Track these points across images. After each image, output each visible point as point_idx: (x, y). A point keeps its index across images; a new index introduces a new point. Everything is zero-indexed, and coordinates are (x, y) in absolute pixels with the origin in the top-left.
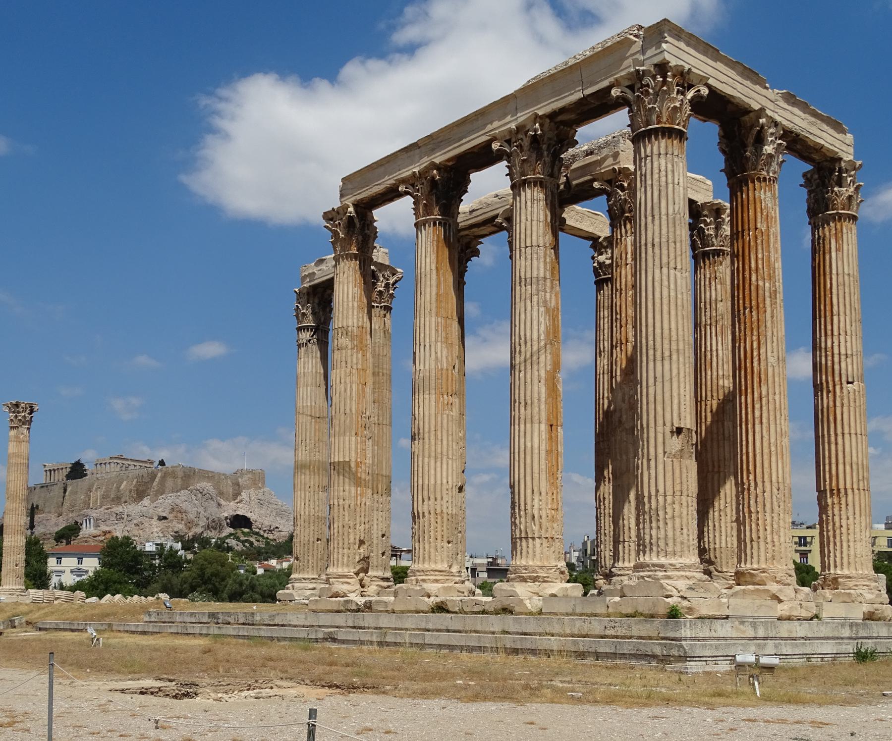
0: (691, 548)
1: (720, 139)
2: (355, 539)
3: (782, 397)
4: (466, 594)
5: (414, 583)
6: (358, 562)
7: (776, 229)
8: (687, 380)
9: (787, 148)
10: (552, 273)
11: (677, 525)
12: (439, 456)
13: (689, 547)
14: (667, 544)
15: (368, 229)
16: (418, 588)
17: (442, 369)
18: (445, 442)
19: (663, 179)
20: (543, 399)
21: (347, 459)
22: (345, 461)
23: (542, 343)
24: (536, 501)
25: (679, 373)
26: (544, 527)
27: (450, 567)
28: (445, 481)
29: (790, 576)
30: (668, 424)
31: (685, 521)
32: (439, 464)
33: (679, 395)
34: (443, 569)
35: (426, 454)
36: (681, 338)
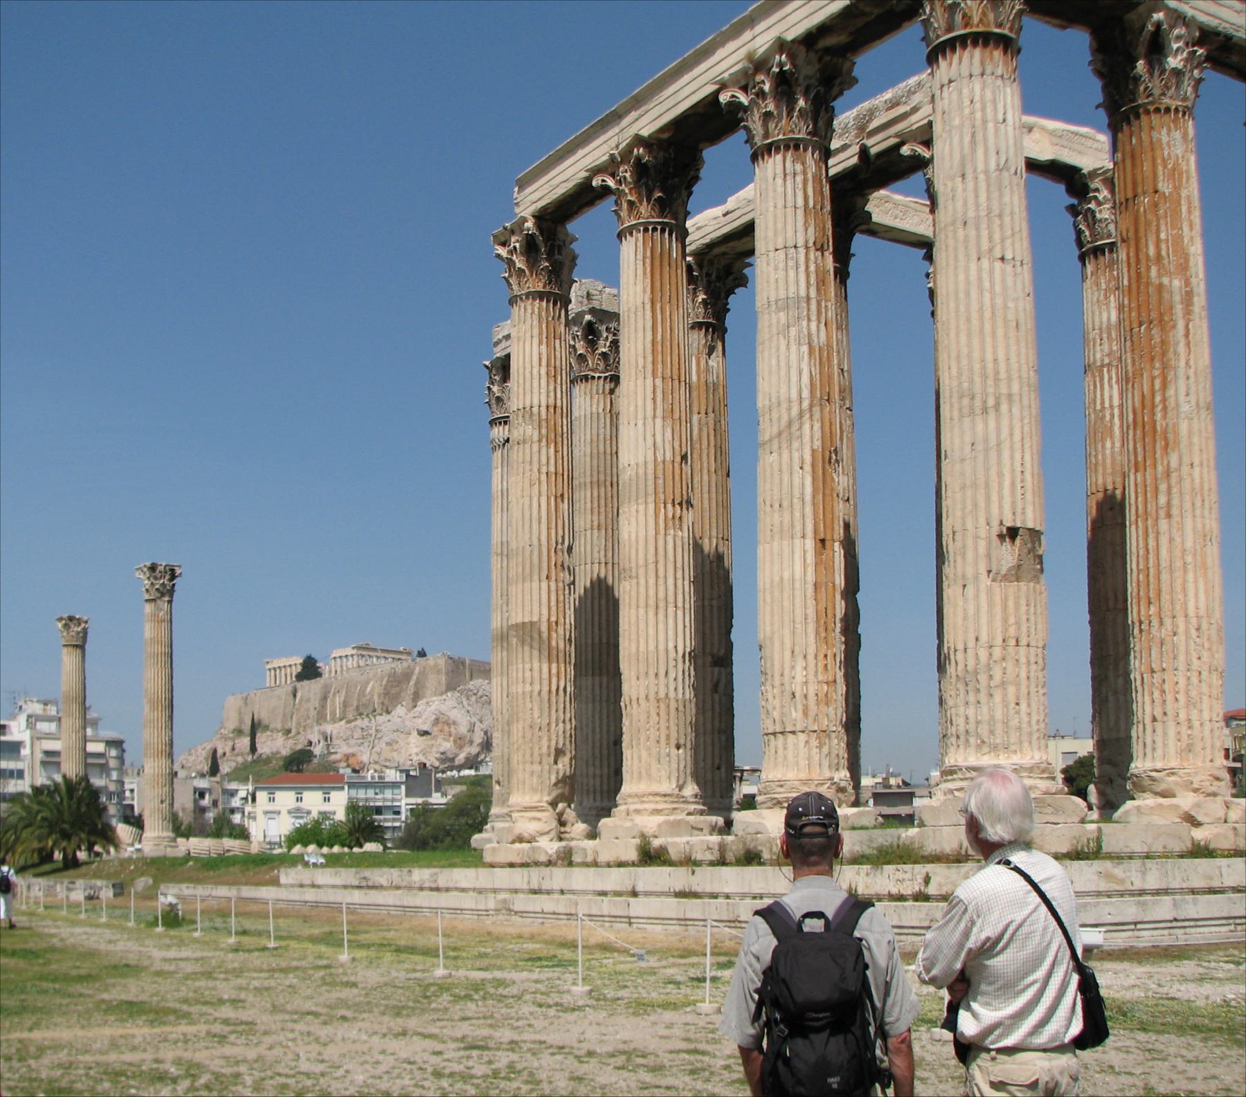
0: (1035, 736)
1: (1093, 54)
2: (549, 747)
3: (1205, 469)
4: (706, 831)
5: (624, 814)
6: (556, 784)
7: (1192, 189)
8: (1027, 446)
9: (1208, 58)
10: (818, 290)
11: (1011, 698)
12: (662, 604)
13: (1030, 734)
14: (992, 732)
15: (560, 253)
16: (628, 824)
17: (664, 462)
18: (671, 581)
19: (978, 115)
20: (808, 498)
21: (535, 619)
22: (532, 623)
23: (806, 404)
24: (799, 668)
25: (1011, 435)
26: (812, 714)
27: (681, 788)
28: (671, 645)
29: (1218, 779)
30: (995, 523)
31: (1024, 690)
32: (661, 616)
33: (1013, 471)
34: (669, 791)
35: (642, 603)
36: (1015, 375)
